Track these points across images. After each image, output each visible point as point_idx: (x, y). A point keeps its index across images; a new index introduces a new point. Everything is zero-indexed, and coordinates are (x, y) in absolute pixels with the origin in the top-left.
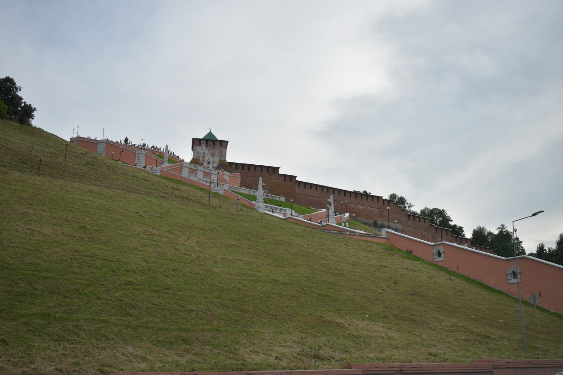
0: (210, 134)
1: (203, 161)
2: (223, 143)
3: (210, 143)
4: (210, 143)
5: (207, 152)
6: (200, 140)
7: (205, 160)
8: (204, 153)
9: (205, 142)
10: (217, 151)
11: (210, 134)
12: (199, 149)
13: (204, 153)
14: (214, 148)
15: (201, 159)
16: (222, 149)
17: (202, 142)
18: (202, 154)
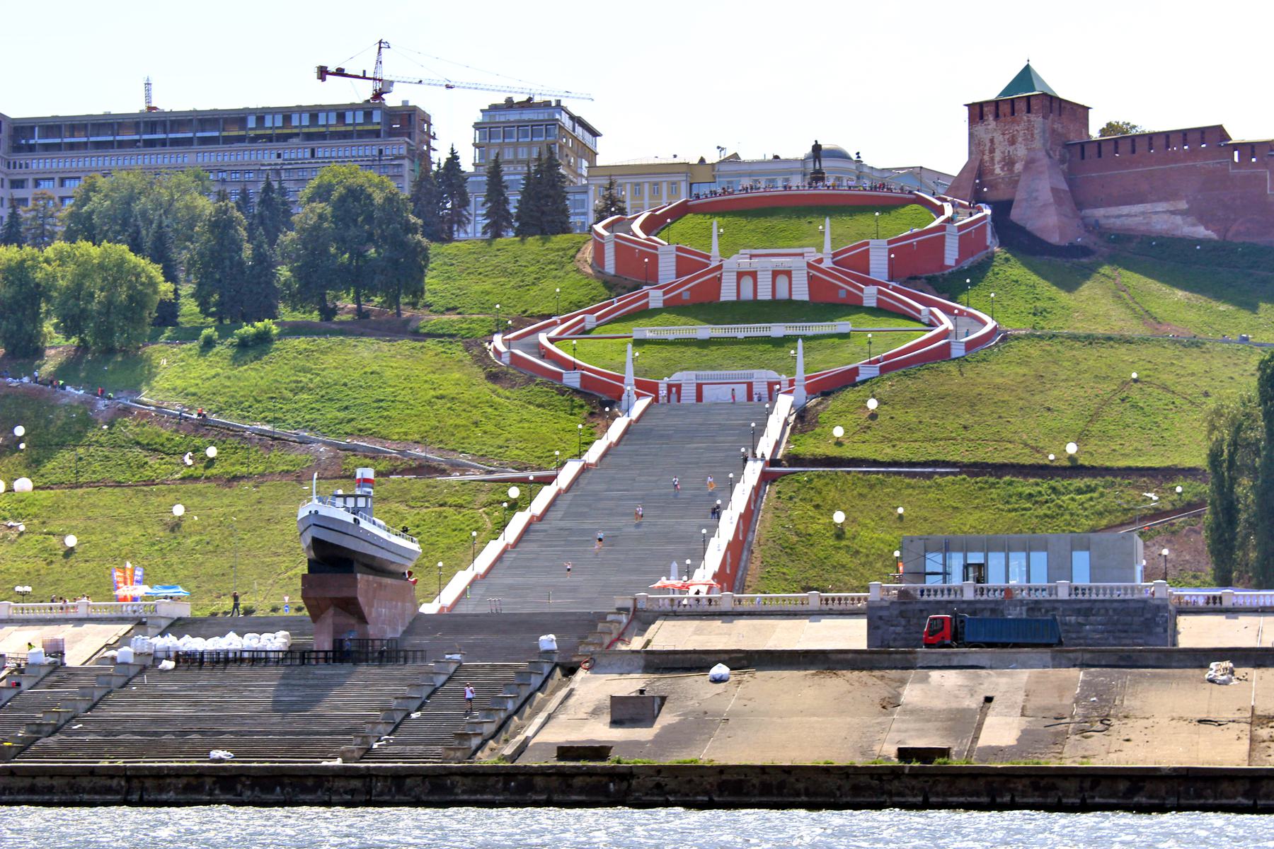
0: (1027, 70)
1: (992, 159)
2: (1033, 102)
3: (1005, 109)
4: (1005, 109)
5: (998, 138)
6: (981, 105)
7: (997, 159)
8: (992, 141)
9: (993, 108)
10: (1020, 129)
11: (1027, 70)
12: (980, 128)
13: (992, 141)
14: (1013, 122)
15: (986, 158)
16: (1032, 117)
17: (985, 109)
18: (988, 145)
